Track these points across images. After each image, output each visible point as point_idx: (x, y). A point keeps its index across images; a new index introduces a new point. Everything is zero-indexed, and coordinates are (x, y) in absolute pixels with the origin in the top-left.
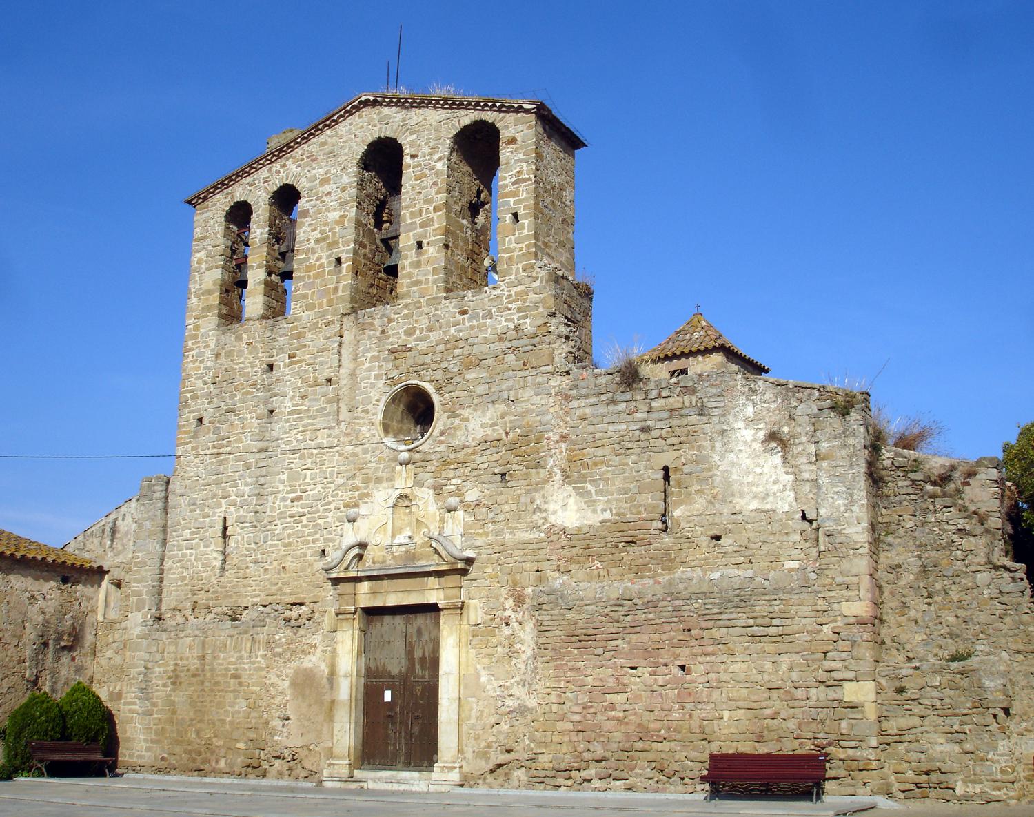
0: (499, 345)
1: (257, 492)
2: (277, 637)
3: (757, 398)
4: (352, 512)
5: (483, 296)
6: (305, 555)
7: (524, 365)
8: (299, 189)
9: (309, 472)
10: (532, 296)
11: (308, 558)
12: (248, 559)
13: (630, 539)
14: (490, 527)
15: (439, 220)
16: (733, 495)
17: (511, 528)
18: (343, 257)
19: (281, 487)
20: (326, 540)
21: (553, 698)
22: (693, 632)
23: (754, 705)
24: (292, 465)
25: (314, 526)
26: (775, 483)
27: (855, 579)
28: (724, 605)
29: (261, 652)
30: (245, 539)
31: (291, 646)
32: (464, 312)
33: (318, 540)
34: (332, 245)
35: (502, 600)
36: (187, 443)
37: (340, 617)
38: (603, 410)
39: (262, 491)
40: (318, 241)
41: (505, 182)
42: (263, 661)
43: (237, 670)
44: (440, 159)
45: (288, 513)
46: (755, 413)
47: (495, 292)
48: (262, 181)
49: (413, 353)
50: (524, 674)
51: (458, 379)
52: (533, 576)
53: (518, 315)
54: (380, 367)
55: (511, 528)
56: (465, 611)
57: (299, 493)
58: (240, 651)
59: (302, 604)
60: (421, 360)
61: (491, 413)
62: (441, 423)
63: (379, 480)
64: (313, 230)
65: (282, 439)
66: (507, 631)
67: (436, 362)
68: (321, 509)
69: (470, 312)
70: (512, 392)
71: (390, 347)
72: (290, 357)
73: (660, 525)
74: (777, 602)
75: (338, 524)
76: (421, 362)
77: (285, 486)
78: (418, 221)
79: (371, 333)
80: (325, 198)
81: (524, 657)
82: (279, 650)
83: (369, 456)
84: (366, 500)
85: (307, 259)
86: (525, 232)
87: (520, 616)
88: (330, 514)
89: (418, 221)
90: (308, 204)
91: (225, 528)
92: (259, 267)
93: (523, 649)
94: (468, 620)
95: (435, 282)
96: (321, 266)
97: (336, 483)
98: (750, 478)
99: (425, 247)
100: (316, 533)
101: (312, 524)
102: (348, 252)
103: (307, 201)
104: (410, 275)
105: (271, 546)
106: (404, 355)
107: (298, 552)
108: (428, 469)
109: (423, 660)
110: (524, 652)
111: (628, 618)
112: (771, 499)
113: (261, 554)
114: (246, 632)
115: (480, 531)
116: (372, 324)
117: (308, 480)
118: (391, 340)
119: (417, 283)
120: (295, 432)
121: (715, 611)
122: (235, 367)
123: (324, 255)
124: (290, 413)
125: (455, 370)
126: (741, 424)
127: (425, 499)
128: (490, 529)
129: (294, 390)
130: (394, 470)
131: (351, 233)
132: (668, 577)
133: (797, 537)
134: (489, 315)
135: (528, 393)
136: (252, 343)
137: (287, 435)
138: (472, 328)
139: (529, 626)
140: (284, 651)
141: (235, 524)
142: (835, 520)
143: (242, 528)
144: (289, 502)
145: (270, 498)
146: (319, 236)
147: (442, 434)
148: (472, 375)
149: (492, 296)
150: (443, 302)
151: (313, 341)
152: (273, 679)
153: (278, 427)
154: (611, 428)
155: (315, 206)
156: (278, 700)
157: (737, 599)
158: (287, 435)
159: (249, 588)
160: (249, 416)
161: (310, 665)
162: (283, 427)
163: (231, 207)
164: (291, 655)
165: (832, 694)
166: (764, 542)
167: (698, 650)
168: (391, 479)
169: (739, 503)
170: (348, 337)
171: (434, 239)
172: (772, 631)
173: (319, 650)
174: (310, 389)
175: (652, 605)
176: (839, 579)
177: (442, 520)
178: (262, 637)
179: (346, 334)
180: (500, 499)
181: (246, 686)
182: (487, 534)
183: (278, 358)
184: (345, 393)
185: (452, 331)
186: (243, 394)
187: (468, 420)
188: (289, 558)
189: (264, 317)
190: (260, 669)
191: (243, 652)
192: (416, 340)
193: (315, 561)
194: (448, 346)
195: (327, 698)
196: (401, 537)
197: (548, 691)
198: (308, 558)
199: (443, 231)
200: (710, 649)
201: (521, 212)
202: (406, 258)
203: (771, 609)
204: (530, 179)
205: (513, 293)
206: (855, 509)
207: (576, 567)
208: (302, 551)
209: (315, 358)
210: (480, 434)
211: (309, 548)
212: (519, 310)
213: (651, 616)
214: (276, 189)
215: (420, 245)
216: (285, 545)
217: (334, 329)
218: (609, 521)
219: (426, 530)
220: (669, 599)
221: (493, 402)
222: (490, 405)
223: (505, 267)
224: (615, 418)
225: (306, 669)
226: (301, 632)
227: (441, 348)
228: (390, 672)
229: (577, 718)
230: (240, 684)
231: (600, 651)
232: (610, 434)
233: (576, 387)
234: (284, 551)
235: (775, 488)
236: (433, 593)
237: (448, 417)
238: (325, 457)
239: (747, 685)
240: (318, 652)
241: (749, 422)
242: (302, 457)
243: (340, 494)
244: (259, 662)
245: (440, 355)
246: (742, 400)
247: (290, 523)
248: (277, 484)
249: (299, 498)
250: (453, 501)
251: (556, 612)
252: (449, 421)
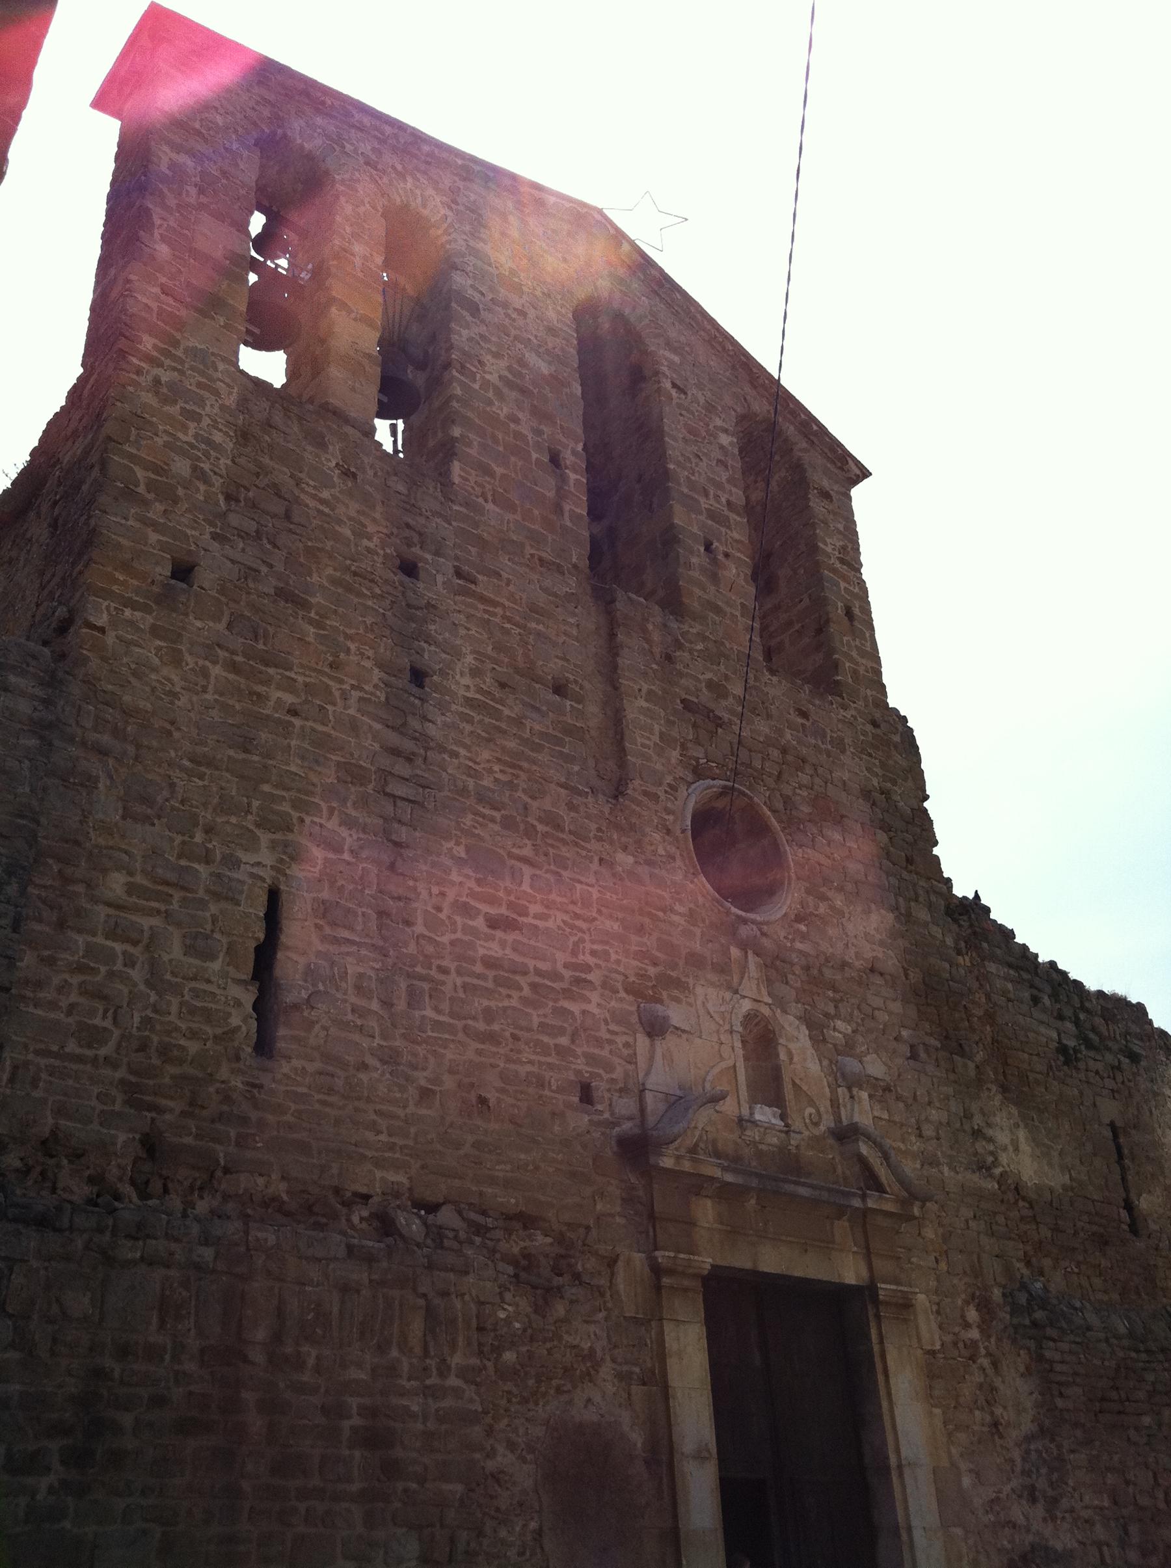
11: (547, 1092)
12: (365, 1043)
29: (456, 1360)
36: (134, 606)
42: (470, 1391)
45: (481, 952)
58: (382, 1348)
75: (613, 1027)
84: (676, 993)
88: (595, 997)
129: (480, 656)
144: (479, 923)
147: (799, 919)
161: (590, 1416)
173: (606, 1371)
191: (395, 1353)
208: (529, 1068)
211: (551, 1066)
234: (479, 1052)
244: (457, 1393)
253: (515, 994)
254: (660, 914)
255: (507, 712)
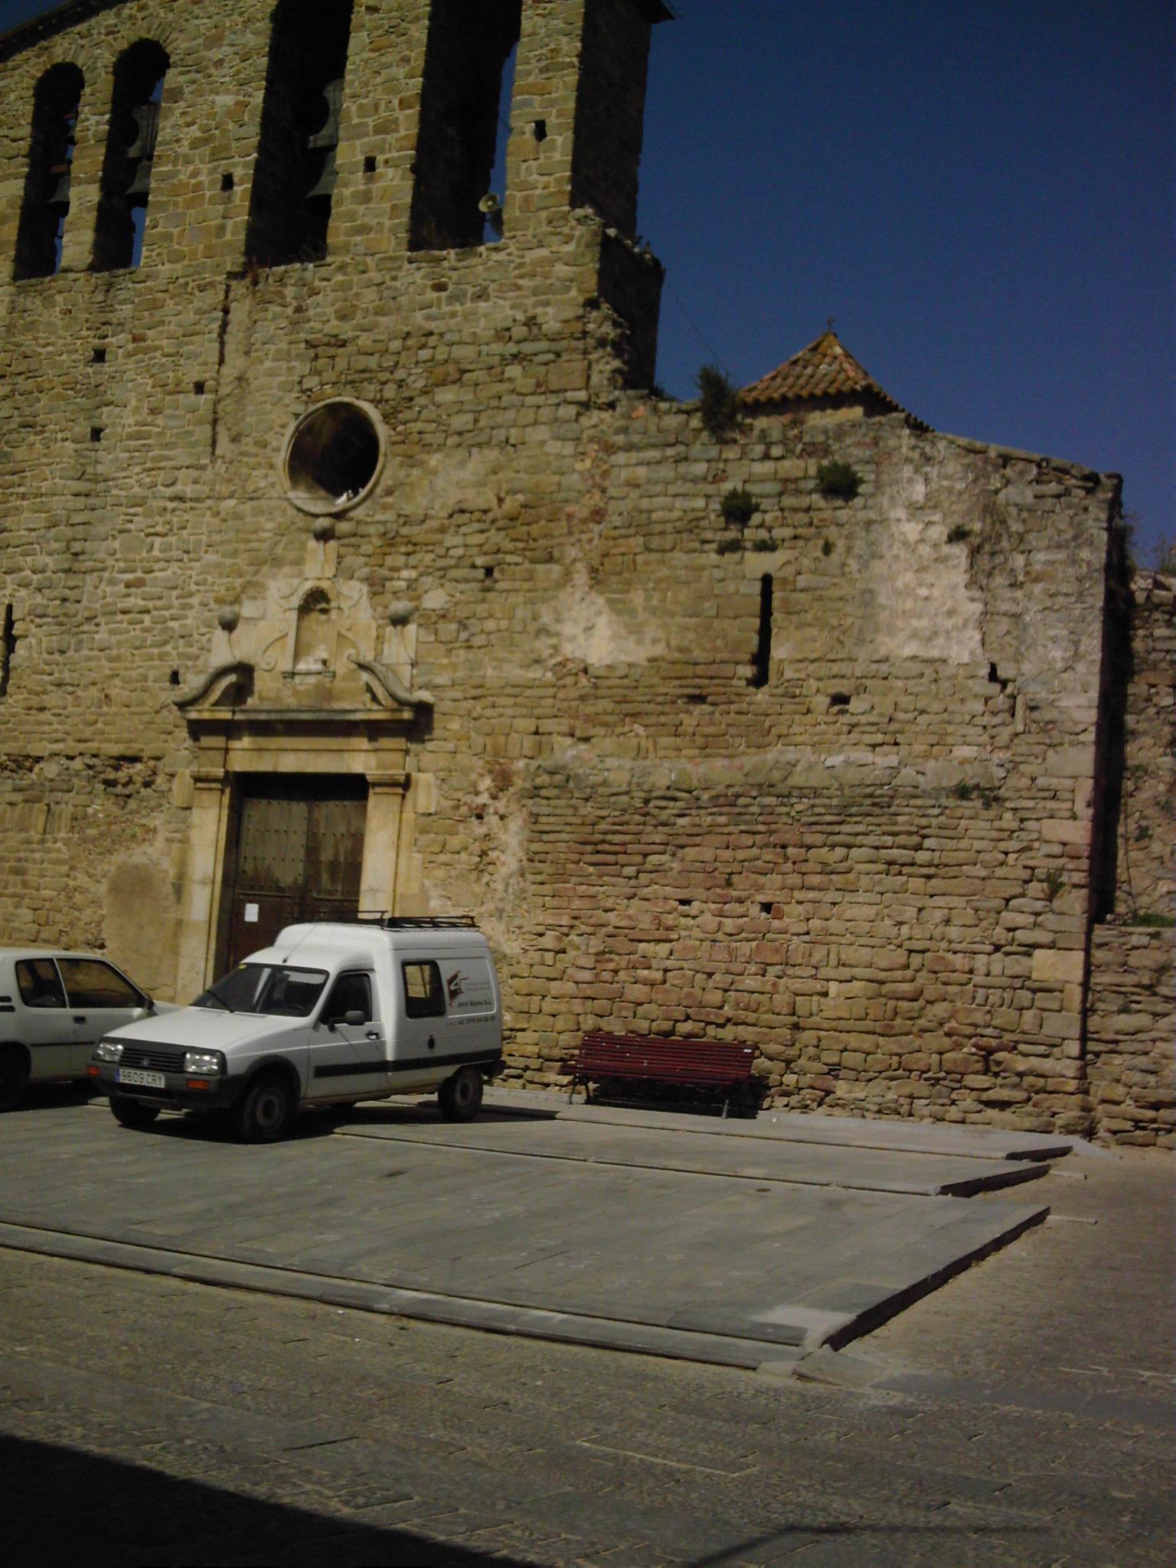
0: (497, 348)
1: (66, 566)
2: (90, 810)
3: (933, 471)
4: (227, 611)
5: (475, 261)
6: (145, 679)
7: (538, 385)
8: (168, 50)
9: (158, 540)
10: (561, 270)
12: (46, 678)
13: (697, 692)
14: (462, 654)
15: (408, 124)
16: (877, 630)
17: (496, 659)
18: (238, 173)
19: (110, 562)
20: (181, 656)
21: (548, 941)
22: (790, 851)
23: (882, 975)
24: (129, 526)
25: (163, 631)
26: (950, 613)
27: (1069, 783)
28: (844, 813)
30: (44, 645)
31: (114, 827)
32: (440, 287)
33: (167, 654)
34: (216, 155)
35: (474, 776)
37: (199, 785)
38: (667, 472)
39: (76, 566)
40: (195, 144)
41: (529, 67)
42: (64, 848)
43: (19, 860)
44: (417, 19)
46: (928, 496)
47: (495, 256)
48: (103, 31)
49: (350, 349)
50: (502, 900)
51: (422, 400)
52: (529, 742)
53: (533, 299)
54: (291, 369)
55: (496, 659)
56: (409, 795)
57: (139, 574)
59: (135, 759)
60: (362, 362)
61: (479, 462)
62: (387, 473)
63: (277, 562)
64: (189, 125)
65: (113, 479)
66: (480, 830)
67: (386, 369)
68: (176, 603)
69: (451, 287)
70: (513, 431)
71: (310, 337)
72: (135, 340)
73: (748, 671)
74: (936, 811)
75: (204, 630)
76: (360, 367)
77: (117, 560)
78: (371, 121)
79: (278, 309)
80: (212, 71)
81: (503, 871)
82: (92, 832)
83: (262, 520)
85: (173, 174)
86: (557, 156)
87: (501, 805)
88: (191, 613)
89: (371, 121)
90: (182, 79)
91: (10, 623)
92: (89, 181)
93: (503, 858)
94: (415, 805)
95: (393, 230)
96: (199, 186)
97: (204, 561)
98: (909, 604)
99: (380, 169)
100: (165, 643)
101: (159, 626)
102: (245, 165)
103: (182, 73)
104: (352, 216)
105: (88, 659)
106: (332, 351)
107: (134, 674)
108: (366, 548)
109: (334, 865)
110: (504, 864)
111: (681, 821)
112: (941, 640)
113: (70, 671)
114: (39, 800)
115: (445, 661)
116: (283, 297)
117: (156, 553)
118: (312, 324)
119: (363, 229)
120: (138, 469)
121: (829, 818)
122: (39, 350)
123: (204, 168)
124: (130, 437)
125: (421, 383)
126: (901, 513)
127: (354, 602)
128: (462, 659)
130: (303, 547)
131: (252, 132)
132: (756, 758)
133: (979, 707)
134: (481, 295)
135: (542, 433)
136: (70, 311)
137: (124, 474)
138: (453, 315)
139: (515, 824)
140: (101, 835)
141: (28, 618)
142: (1045, 683)
143: (40, 626)
144: (121, 588)
145: (88, 578)
146: (199, 134)
148: (447, 395)
149: (491, 263)
150: (406, 266)
151: (178, 314)
152: (81, 879)
153: (108, 458)
154: (679, 503)
155: (194, 82)
156: (88, 914)
157: (868, 801)
158: (124, 474)
159: (46, 728)
160: (59, 436)
162: (117, 459)
163: (47, 72)
164: (114, 842)
165: (1017, 965)
166: (922, 712)
167: (795, 879)
168: (299, 562)
169: (887, 645)
170: (239, 312)
171: (395, 154)
172: (922, 856)
173: (161, 837)
174: (168, 398)
175: (727, 801)
176: (1041, 782)
177: (380, 639)
178: (67, 810)
179: (233, 306)
180: (481, 609)
181: (33, 888)
182: (454, 667)
183: (114, 340)
184: (229, 409)
185: (419, 317)
186: (51, 399)
187: (435, 472)
188: (117, 682)
189: (93, 268)
190: (62, 862)
192: (354, 329)
193: (163, 689)
194: (409, 343)
195: (173, 915)
196: (310, 659)
197: (540, 929)
198: (150, 683)
199: (413, 142)
200: (816, 880)
201: (552, 121)
202: (346, 186)
203: (924, 821)
204: (571, 65)
205: (527, 260)
206: (1081, 667)
207: (601, 731)
208: (139, 670)
209: (180, 345)
210: (452, 499)
211: (152, 667)
212: (535, 292)
213: (723, 819)
214: (125, 45)
215: (370, 165)
216: (111, 660)
217: (215, 297)
218: (663, 659)
219: (352, 651)
220: (754, 794)
221: (479, 445)
222: (475, 450)
223: (518, 213)
224: (688, 487)
225: (136, 867)
226: (132, 804)
227: (396, 345)
228: (277, 881)
229: (586, 975)
230: (25, 884)
231: (630, 871)
232: (676, 514)
233: (625, 430)
235: (949, 623)
236: (358, 759)
237: (401, 465)
238: (186, 517)
239: (872, 942)
240: (160, 842)
241: (915, 510)
242: (149, 513)
243: (210, 580)
244: (59, 851)
245: (395, 358)
246: (907, 471)
247: (121, 622)
248: (102, 555)
249: (140, 583)
250: (400, 606)
251: (563, 802)
252: (402, 473)
253: (138, 627)
254: (253, 537)
255: (157, 430)
